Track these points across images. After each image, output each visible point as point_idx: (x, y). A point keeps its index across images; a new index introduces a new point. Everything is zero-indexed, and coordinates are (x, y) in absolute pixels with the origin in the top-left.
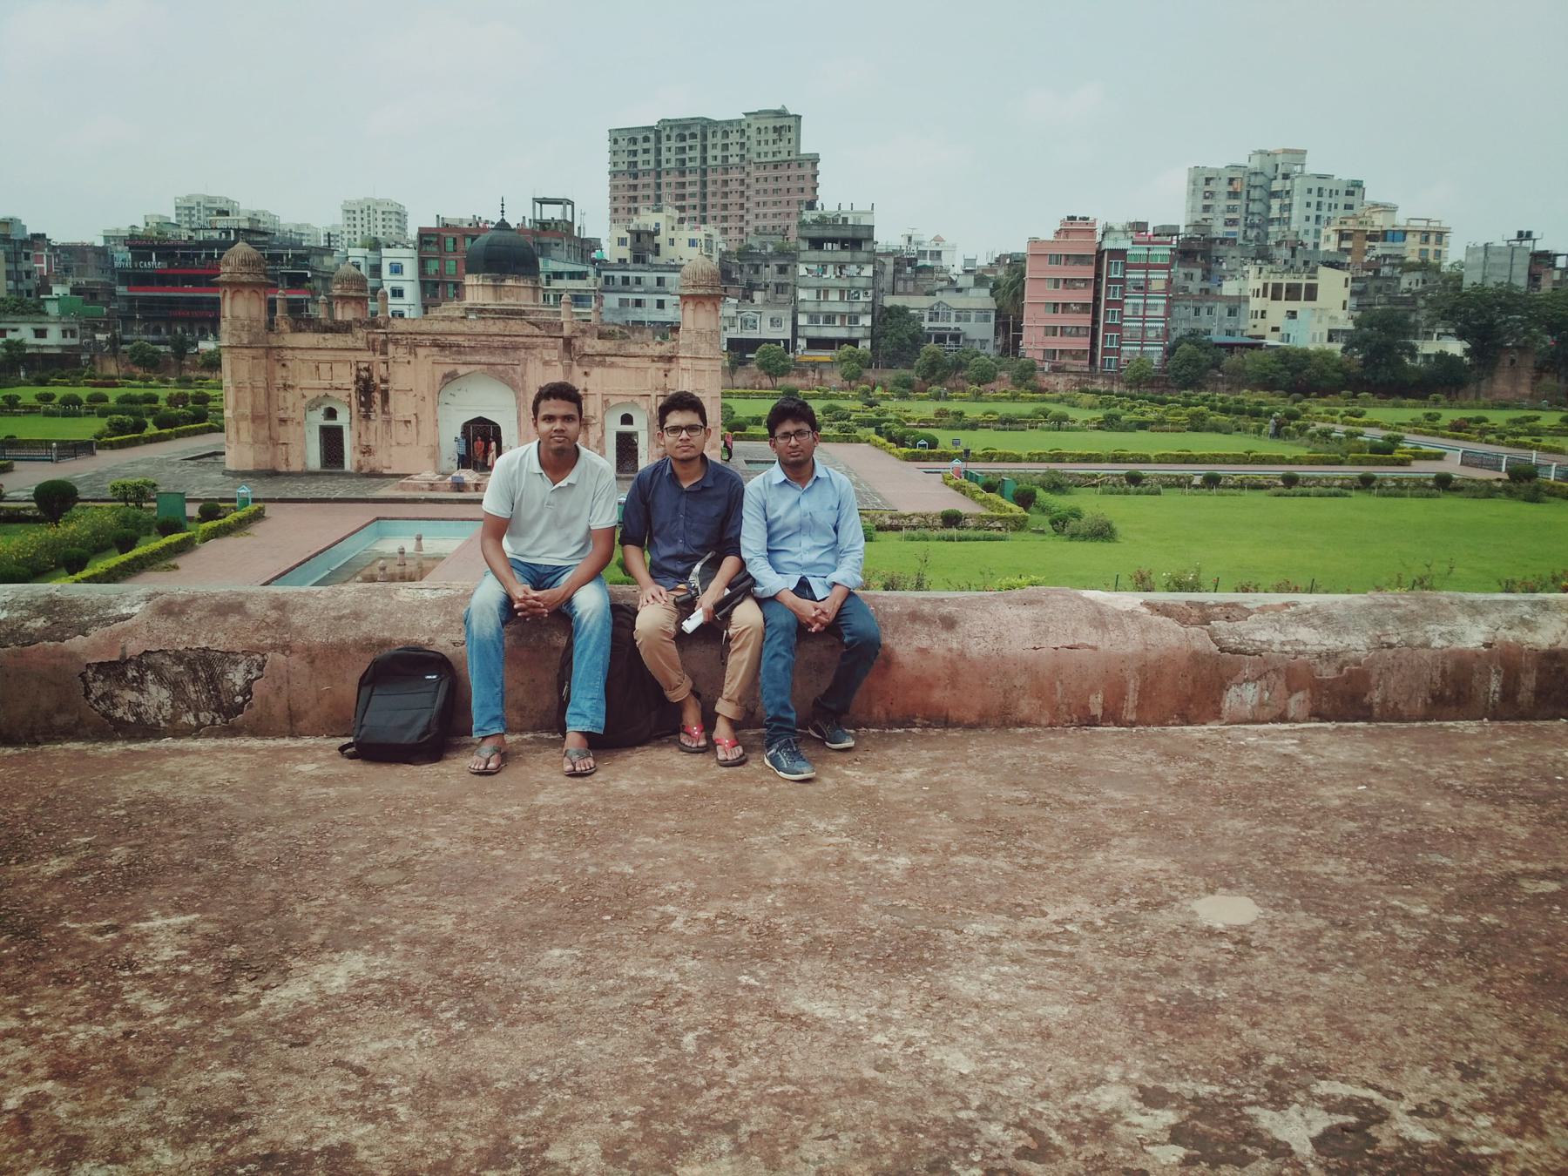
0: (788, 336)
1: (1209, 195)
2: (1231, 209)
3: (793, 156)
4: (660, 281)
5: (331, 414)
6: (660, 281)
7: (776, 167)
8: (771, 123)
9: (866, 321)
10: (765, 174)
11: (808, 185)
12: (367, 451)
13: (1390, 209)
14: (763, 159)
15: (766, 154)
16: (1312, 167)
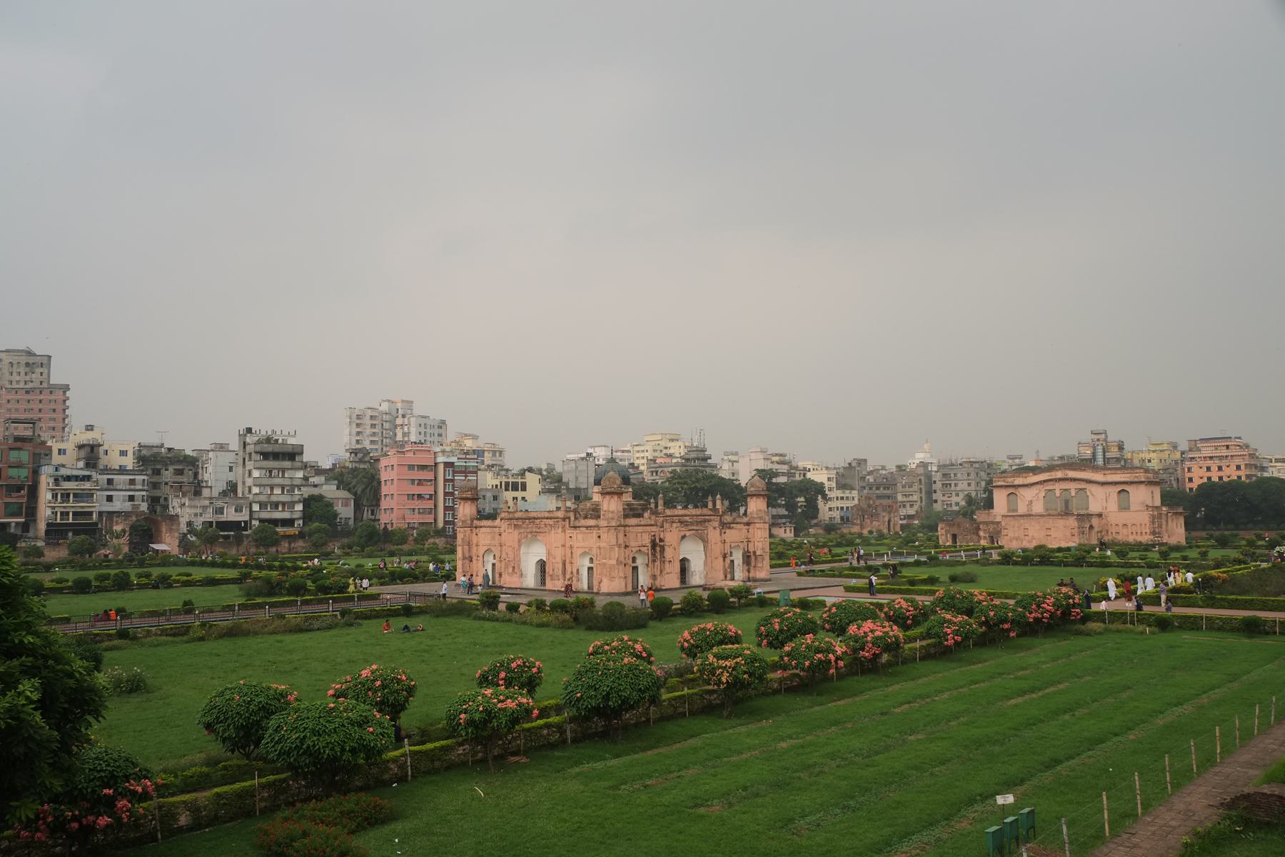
0: (247, 518)
1: (358, 425)
2: (374, 434)
3: (45, 385)
4: (110, 482)
5: (634, 560)
6: (110, 482)
7: (27, 392)
8: (24, 359)
9: (299, 507)
10: (18, 397)
11: (59, 407)
12: (654, 577)
13: (475, 437)
14: (15, 386)
15: (18, 382)
16: (417, 411)
